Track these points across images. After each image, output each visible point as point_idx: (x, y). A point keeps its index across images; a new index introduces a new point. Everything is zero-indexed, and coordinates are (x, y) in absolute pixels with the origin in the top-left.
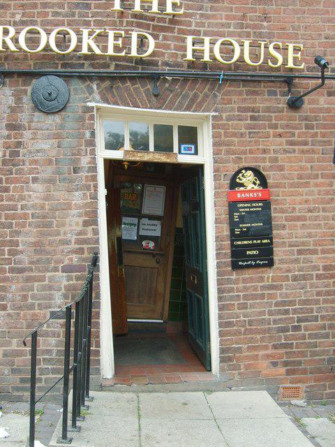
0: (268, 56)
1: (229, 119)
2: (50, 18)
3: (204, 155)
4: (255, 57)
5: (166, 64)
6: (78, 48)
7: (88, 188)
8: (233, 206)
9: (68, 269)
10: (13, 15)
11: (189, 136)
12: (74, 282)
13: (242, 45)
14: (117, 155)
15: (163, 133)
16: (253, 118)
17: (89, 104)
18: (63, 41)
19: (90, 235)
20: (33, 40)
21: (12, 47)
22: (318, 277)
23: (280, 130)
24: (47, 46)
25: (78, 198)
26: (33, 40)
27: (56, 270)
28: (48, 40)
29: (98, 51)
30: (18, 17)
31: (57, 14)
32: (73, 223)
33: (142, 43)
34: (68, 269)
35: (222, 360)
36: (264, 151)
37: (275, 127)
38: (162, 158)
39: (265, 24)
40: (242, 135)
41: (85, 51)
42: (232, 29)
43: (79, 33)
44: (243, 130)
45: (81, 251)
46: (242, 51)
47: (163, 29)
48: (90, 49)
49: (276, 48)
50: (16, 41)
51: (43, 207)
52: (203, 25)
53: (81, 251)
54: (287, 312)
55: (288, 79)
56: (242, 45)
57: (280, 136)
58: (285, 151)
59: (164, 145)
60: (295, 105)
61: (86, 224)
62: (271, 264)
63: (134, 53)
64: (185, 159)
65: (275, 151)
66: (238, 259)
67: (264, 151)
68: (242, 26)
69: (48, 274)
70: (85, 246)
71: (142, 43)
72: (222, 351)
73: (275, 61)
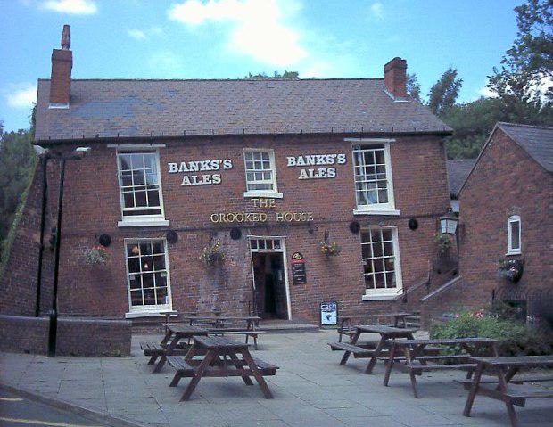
3: (283, 249)
8: (293, 265)
11: (277, 243)
14: (256, 250)
15: (269, 242)
25: (245, 265)
32: (245, 272)
35: (292, 314)
38: (269, 251)
46: (294, 216)
55: (309, 224)
59: (269, 246)
62: (305, 283)
64: (277, 250)
66: (295, 282)
72: (292, 312)
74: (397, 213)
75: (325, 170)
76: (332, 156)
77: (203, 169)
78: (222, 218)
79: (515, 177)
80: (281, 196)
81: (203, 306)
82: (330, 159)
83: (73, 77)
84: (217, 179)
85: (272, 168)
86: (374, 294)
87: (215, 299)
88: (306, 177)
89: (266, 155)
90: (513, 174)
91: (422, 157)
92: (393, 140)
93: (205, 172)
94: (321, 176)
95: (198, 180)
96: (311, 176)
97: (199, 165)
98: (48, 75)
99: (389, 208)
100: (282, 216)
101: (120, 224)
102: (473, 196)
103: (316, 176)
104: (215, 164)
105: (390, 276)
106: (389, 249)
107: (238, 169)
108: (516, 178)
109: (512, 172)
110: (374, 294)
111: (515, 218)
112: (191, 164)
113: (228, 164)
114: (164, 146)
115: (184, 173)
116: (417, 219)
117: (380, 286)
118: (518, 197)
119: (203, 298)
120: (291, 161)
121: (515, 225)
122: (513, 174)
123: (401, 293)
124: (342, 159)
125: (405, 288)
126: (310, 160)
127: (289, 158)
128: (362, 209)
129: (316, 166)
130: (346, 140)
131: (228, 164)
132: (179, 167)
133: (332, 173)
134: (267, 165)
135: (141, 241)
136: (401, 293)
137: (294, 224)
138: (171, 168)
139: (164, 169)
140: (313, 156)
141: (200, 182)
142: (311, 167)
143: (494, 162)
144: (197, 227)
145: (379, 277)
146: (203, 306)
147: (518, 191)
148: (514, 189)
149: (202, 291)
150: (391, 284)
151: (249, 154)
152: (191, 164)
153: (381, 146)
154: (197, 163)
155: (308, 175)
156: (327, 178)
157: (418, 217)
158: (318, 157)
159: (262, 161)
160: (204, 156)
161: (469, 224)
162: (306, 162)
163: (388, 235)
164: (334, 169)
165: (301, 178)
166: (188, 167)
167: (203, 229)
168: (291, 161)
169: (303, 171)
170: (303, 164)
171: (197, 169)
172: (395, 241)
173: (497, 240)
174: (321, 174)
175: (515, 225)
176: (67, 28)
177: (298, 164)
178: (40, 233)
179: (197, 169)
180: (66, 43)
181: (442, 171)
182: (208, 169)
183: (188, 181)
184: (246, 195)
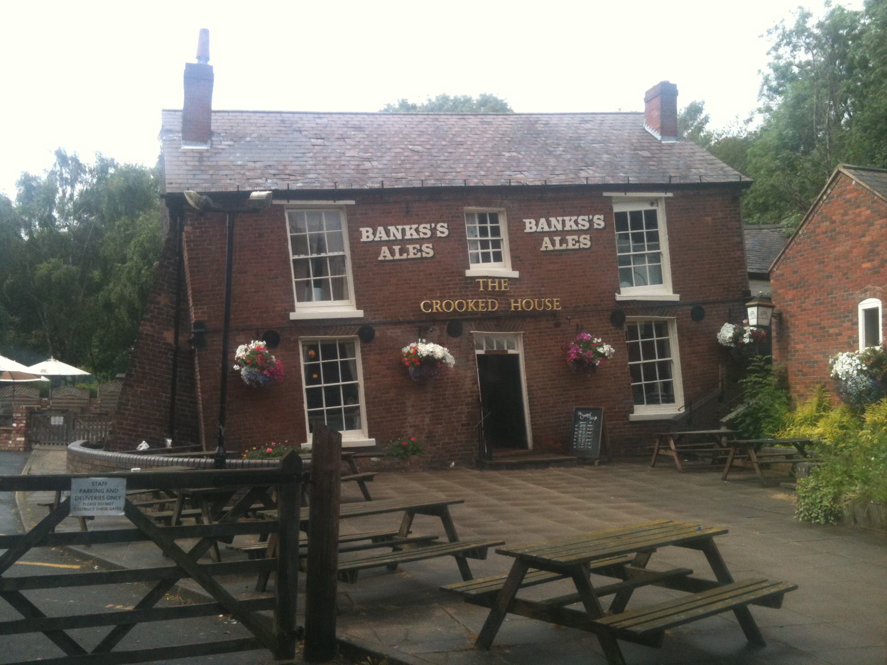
0: (545, 305)
1: (530, 334)
2: (452, 294)
4: (540, 306)
5: (502, 311)
6: (467, 307)
7: (473, 369)
9: (467, 404)
10: (436, 294)
12: (470, 410)
13: (534, 302)
16: (540, 332)
17: (471, 332)
18: (460, 305)
19: (475, 389)
20: (448, 306)
21: (440, 310)
22: (573, 401)
23: (551, 337)
24: (454, 308)
26: (448, 306)
27: (462, 405)
28: (455, 305)
29: (475, 309)
30: (438, 295)
31: (454, 292)
33: (493, 304)
34: (467, 404)
36: (545, 347)
37: (549, 335)
39: (543, 289)
40: (536, 340)
41: (470, 310)
42: (529, 293)
43: (467, 303)
44: (536, 338)
45: (472, 396)
46: (534, 304)
47: (499, 296)
48: (472, 309)
49: (548, 301)
50: (441, 306)
51: (454, 378)
52: (516, 292)
53: (472, 396)
54: (559, 418)
55: (554, 314)
56: (534, 302)
57: (552, 339)
58: (554, 346)
60: (557, 325)
61: (474, 384)
63: (490, 309)
64: (511, 352)
65: (550, 346)
67: (545, 347)
68: (532, 291)
69: (459, 407)
70: (474, 394)
71: (493, 304)
73: (548, 307)
74: (676, 298)
75: (576, 237)
76: (586, 218)
77: (408, 237)
78: (438, 306)
79: (870, 243)
80: (516, 274)
81: (410, 431)
82: (583, 222)
83: (214, 107)
84: (428, 251)
85: (504, 235)
86: (644, 412)
87: (427, 421)
88: (550, 248)
89: (494, 218)
90: (867, 239)
91: (710, 219)
92: (670, 195)
93: (412, 241)
94: (570, 246)
95: (402, 252)
96: (558, 247)
97: (403, 231)
98: (180, 105)
99: (664, 292)
100: (520, 304)
101: (293, 316)
102: (795, 272)
103: (564, 247)
104: (425, 230)
105: (668, 388)
106: (664, 349)
107: (457, 234)
108: (874, 244)
109: (864, 236)
110: (644, 412)
111: (873, 303)
112: (392, 229)
113: (443, 230)
114: (353, 202)
115: (382, 243)
116: (704, 307)
117: (653, 400)
118: (876, 272)
119: (410, 419)
120: (530, 226)
121: (871, 314)
122: (867, 239)
123: (683, 411)
124: (599, 221)
125: (688, 403)
126: (556, 223)
127: (527, 221)
128: (629, 293)
129: (563, 234)
130: (605, 194)
131: (443, 230)
132: (374, 234)
133: (585, 242)
134: (496, 231)
135: (322, 341)
136: (683, 411)
137: (534, 316)
138: (364, 234)
139: (354, 236)
140: (560, 219)
141: (405, 256)
142: (556, 233)
143: (833, 222)
144: (401, 319)
145: (651, 388)
146: (410, 431)
147: (876, 263)
148: (869, 261)
149: (410, 410)
150: (669, 398)
151: (470, 215)
152: (392, 229)
153: (654, 201)
154: (400, 227)
155: (553, 244)
156: (580, 249)
157: (704, 303)
158: (567, 219)
159: (489, 225)
160: (408, 217)
161: (787, 312)
162: (550, 226)
163: (662, 329)
164: (588, 237)
165: (543, 249)
166: (388, 233)
167: (410, 322)
168: (530, 226)
169: (547, 239)
170: (546, 229)
171: (399, 236)
172: (673, 338)
173: (840, 334)
174: (570, 243)
175: (871, 314)
176: (205, 33)
177: (539, 230)
178: (173, 331)
179: (399, 236)
180: (204, 54)
181: (737, 239)
182: (415, 236)
183: (388, 254)
184: (469, 273)
